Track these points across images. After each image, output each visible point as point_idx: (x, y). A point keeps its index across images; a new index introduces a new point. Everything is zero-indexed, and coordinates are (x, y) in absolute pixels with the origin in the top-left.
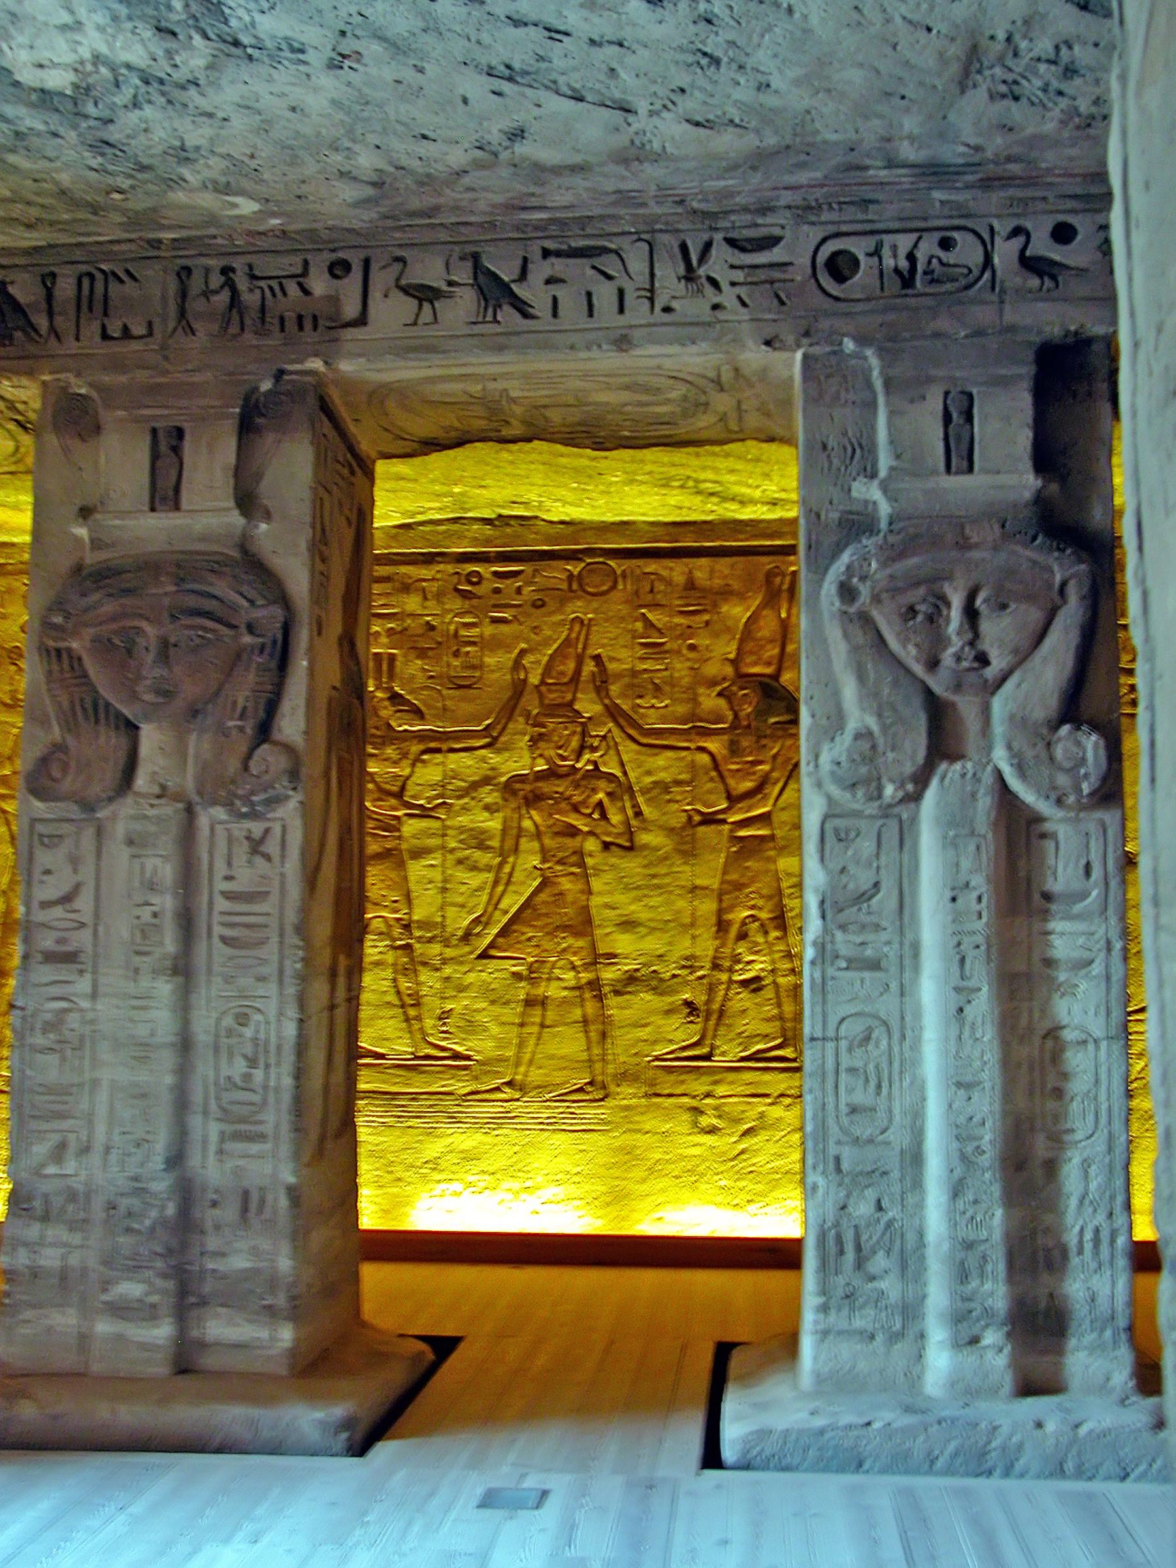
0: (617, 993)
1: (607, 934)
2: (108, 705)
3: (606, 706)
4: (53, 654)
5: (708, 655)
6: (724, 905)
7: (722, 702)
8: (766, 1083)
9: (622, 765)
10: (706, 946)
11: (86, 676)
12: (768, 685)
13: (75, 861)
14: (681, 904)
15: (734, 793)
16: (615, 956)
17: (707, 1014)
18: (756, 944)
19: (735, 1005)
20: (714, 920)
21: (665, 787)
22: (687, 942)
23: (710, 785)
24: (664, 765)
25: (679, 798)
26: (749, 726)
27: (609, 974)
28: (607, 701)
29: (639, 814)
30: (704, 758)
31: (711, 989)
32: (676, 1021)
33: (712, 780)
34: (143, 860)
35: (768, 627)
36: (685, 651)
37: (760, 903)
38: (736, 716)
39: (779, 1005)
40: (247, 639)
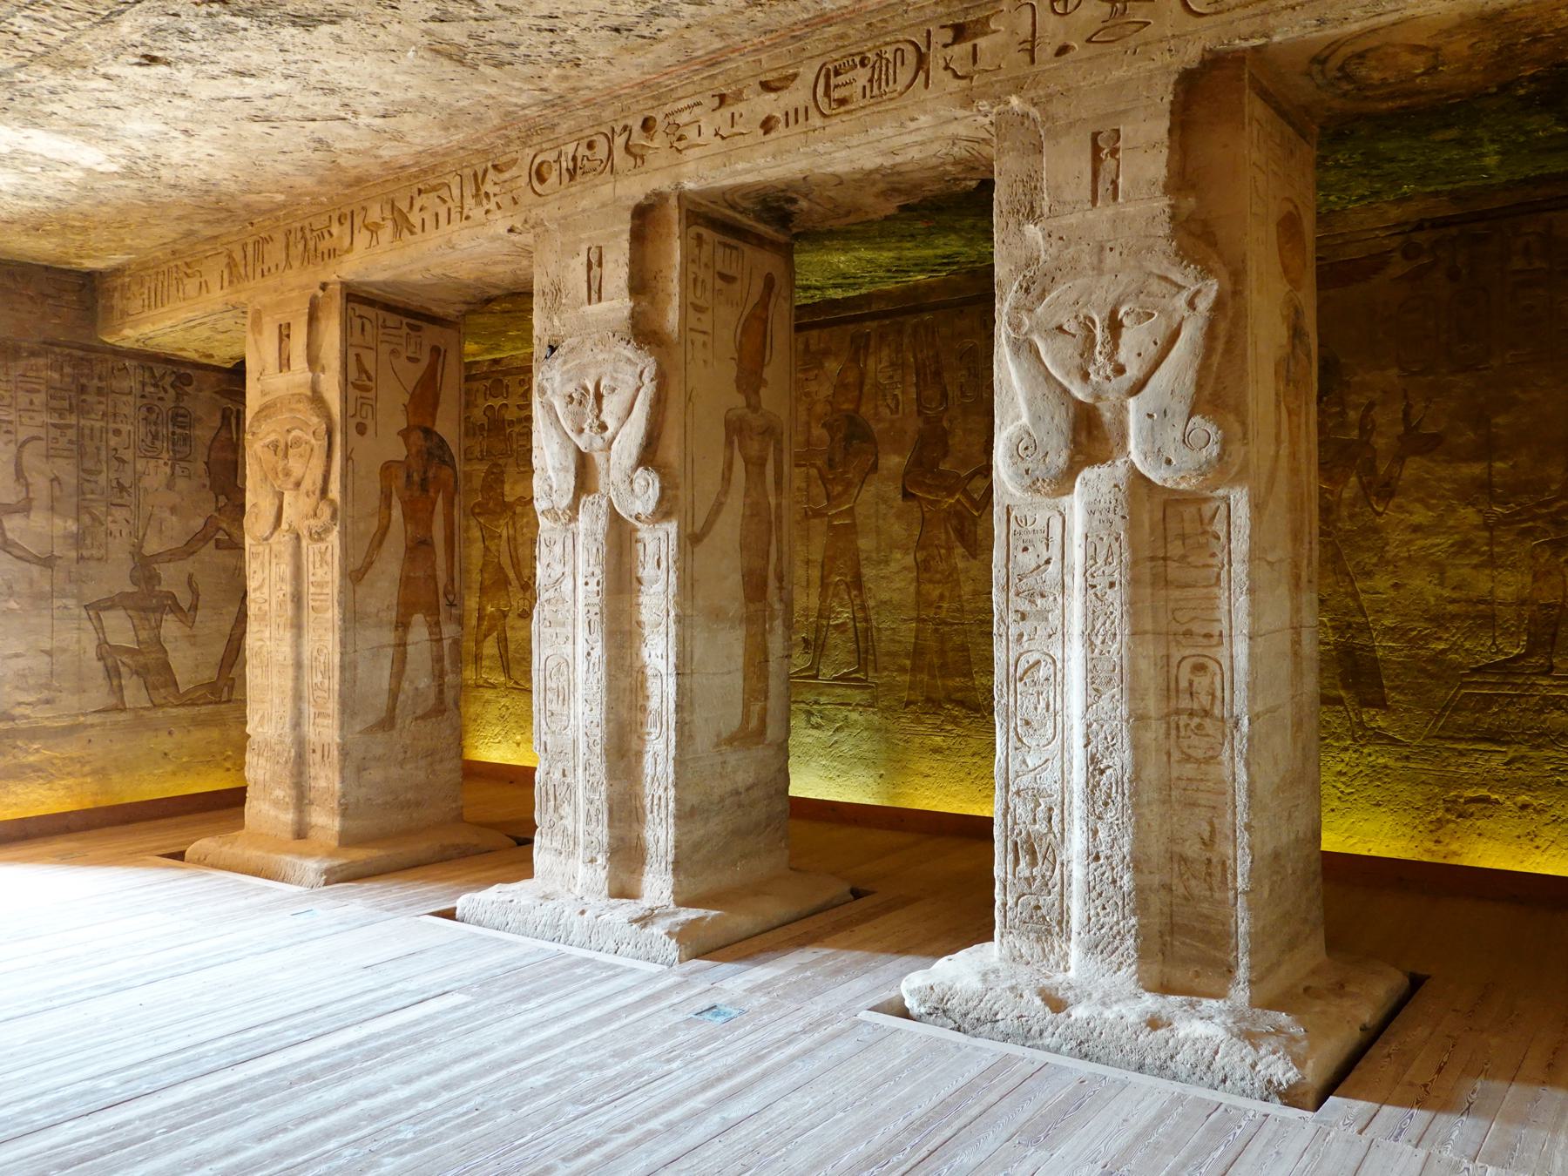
7: (824, 432)
31: (818, 630)
38: (832, 440)
39: (857, 642)
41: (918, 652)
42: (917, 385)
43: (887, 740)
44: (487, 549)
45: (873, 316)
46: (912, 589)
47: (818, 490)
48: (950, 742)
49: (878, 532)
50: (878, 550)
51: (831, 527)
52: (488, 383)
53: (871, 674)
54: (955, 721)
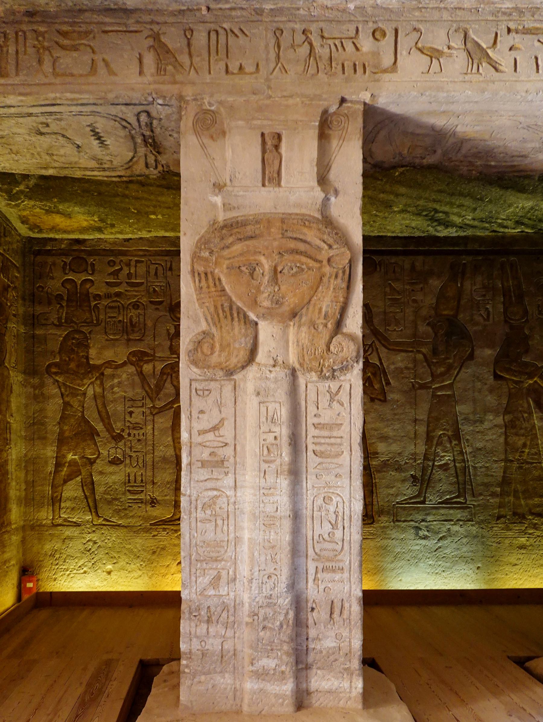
0: (378, 471)
1: (374, 443)
2: (238, 308)
3: (371, 330)
4: (203, 276)
6: (430, 428)
7: (430, 329)
8: (451, 514)
9: (380, 360)
10: (421, 449)
11: (224, 290)
13: (220, 406)
14: (409, 427)
16: (377, 453)
17: (423, 481)
18: (446, 447)
20: (425, 436)
22: (413, 447)
24: (400, 360)
25: (408, 376)
27: (374, 463)
28: (372, 328)
29: (388, 383)
31: (424, 470)
32: (408, 484)
33: (424, 367)
34: (268, 404)
36: (411, 303)
39: (457, 476)
40: (327, 269)
41: (505, 482)
42: (504, 303)
43: (483, 543)
44: (66, 404)
46: (502, 440)
47: (423, 369)
48: (532, 541)
49: (474, 401)
50: (474, 413)
51: (434, 396)
52: (68, 260)
53: (469, 498)
54: (535, 527)
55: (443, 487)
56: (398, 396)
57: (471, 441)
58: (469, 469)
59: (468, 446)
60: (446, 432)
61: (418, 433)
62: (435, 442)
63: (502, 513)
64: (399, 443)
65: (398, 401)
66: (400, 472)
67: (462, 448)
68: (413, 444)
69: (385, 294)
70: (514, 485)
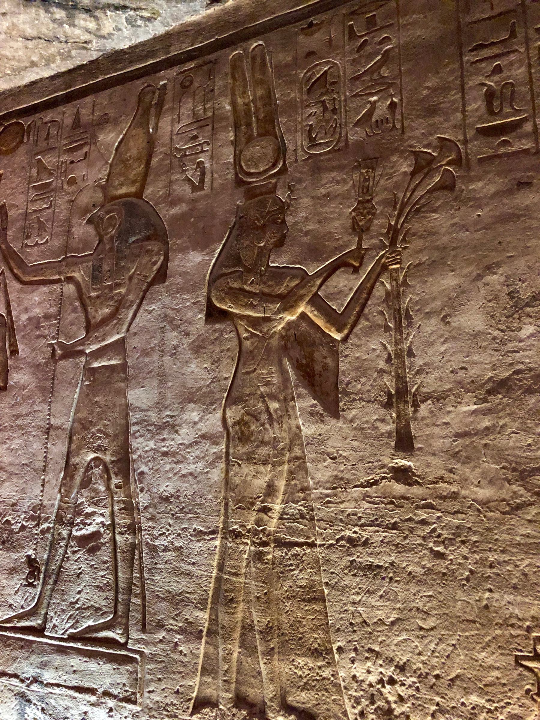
5: (82, 185)
6: (74, 446)
7: (91, 229)
12: (132, 203)
15: (93, 321)
19: (72, 567)
21: (36, 323)
22: (37, 490)
23: (73, 315)
25: (47, 332)
26: (111, 249)
29: (15, 352)
30: (70, 289)
31: (53, 546)
32: (17, 581)
33: (74, 310)
35: (136, 148)
36: (66, 186)
37: (105, 442)
45: (170, 63)
46: (216, 475)
49: (162, 377)
50: (160, 406)
53: (135, 634)
55: (83, 596)
56: (26, 377)
57: (148, 478)
58: (141, 553)
59: (142, 490)
60: (99, 455)
61: (50, 456)
62: (78, 479)
63: (209, 692)
64: (15, 481)
65: (25, 387)
66: (8, 550)
67: (129, 496)
68: (40, 482)
69: (30, 179)
70: (242, 606)
